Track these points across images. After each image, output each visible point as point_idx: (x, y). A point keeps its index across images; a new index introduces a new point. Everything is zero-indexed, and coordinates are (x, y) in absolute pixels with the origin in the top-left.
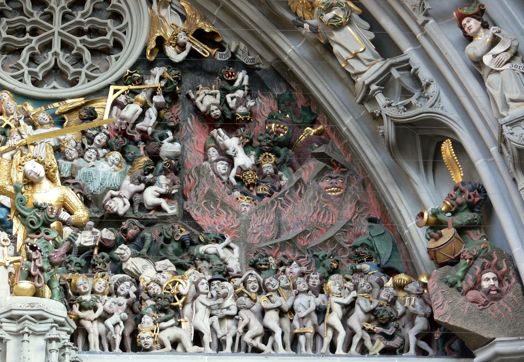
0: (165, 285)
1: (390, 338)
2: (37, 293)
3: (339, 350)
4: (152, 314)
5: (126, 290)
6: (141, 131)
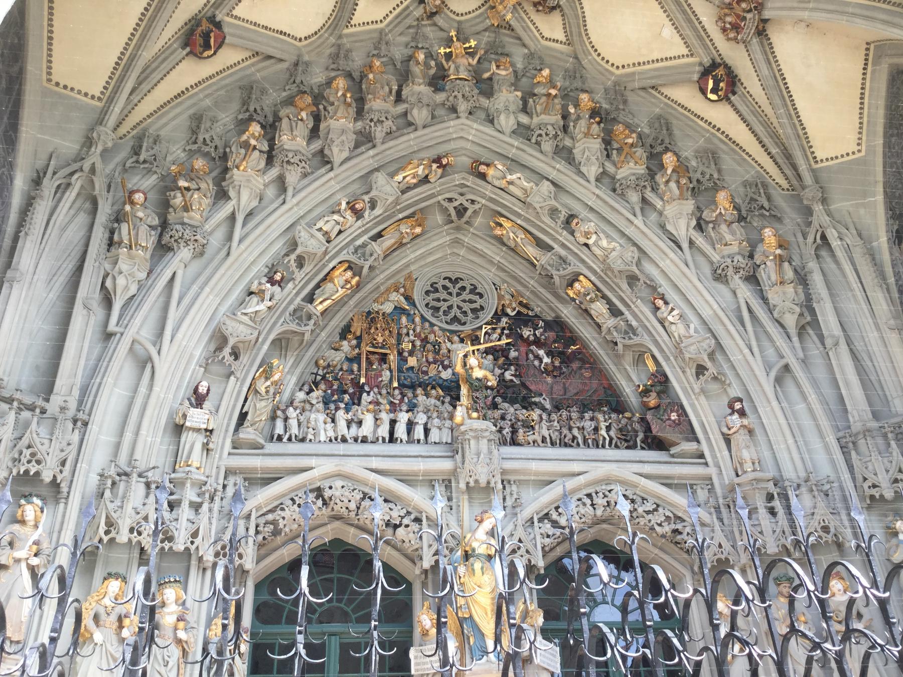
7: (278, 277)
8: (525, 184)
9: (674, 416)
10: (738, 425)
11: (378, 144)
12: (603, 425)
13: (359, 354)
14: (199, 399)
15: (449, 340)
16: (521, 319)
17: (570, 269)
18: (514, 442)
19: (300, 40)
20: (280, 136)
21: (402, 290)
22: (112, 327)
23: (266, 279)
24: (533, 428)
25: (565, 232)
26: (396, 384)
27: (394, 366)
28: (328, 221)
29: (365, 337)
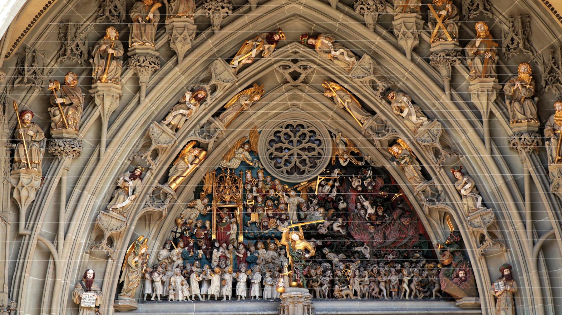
0: (343, 272)
1: (426, 292)
2: (299, 286)
3: (407, 298)
4: (339, 284)
5: (329, 275)
6: (330, 198)
7: (138, 172)
8: (348, 59)
9: (461, 274)
10: (502, 290)
11: (216, 32)
12: (406, 279)
13: (211, 211)
14: (87, 285)
17: (388, 136)
18: (331, 295)
20: (132, 43)
21: (247, 147)
22: (22, 231)
23: (128, 174)
24: (348, 283)
25: (384, 102)
26: (241, 238)
27: (240, 221)
28: (175, 116)
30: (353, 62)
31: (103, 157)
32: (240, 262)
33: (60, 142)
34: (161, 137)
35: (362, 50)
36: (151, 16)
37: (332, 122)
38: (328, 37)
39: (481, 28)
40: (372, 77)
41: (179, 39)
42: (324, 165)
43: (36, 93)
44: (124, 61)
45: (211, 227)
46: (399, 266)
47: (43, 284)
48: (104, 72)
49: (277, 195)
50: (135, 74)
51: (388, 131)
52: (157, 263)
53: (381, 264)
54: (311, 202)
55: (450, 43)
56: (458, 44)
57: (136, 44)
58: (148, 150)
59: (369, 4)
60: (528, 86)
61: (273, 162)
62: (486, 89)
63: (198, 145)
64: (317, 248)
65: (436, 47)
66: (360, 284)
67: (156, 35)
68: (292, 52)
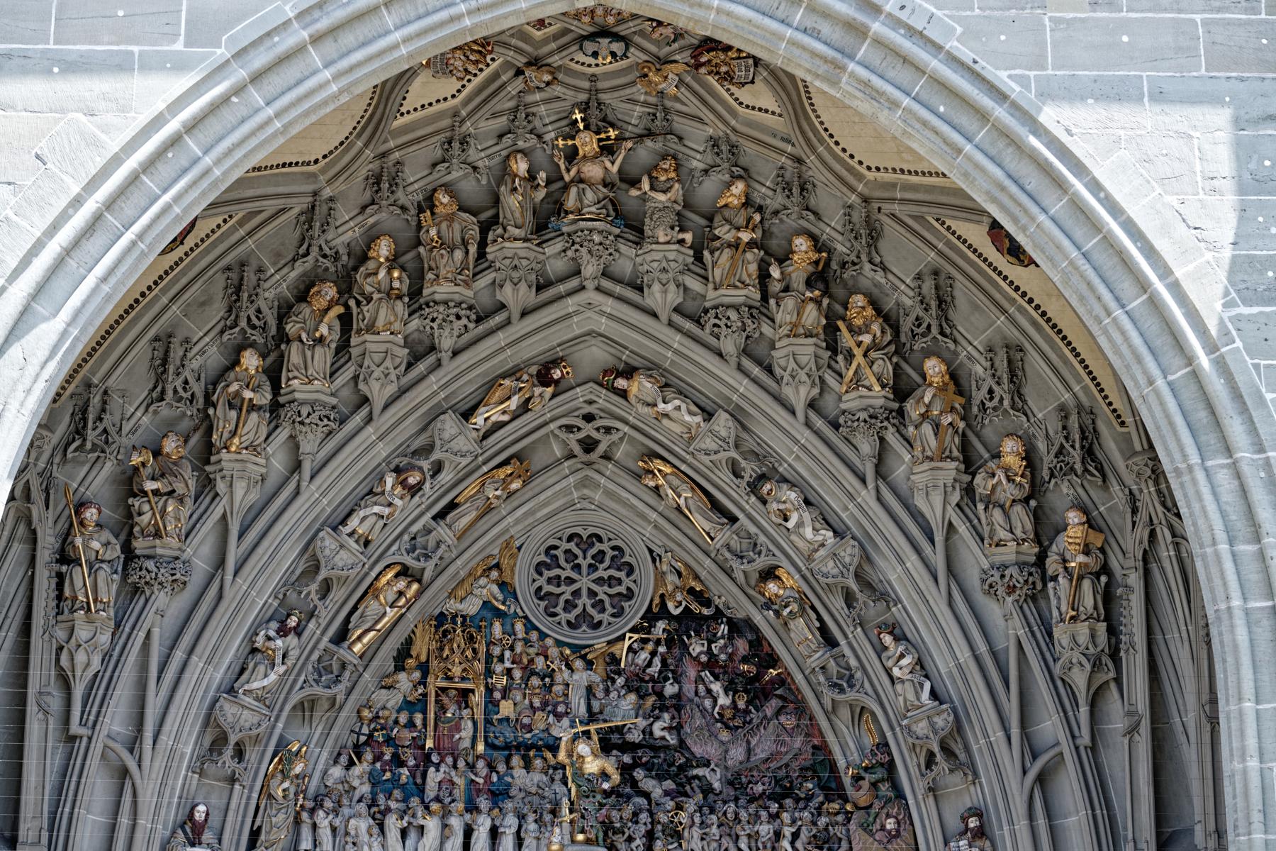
2: (588, 842)
7: (292, 622)
8: (688, 418)
9: (890, 824)
11: (445, 362)
12: (788, 831)
13: (425, 695)
15: (569, 667)
16: (689, 622)
17: (762, 562)
19: (316, 161)
20: (289, 379)
22: (75, 728)
23: (274, 625)
25: (753, 499)
26: (481, 747)
27: (480, 716)
29: (434, 663)
30: (698, 425)
31: (228, 593)
32: (479, 791)
33: (150, 564)
34: (338, 557)
35: (715, 403)
36: (324, 330)
37: (654, 532)
38: (651, 376)
39: (934, 367)
40: (734, 454)
41: (375, 375)
42: (637, 612)
43: (109, 467)
44: (271, 412)
45: (425, 725)
46: (774, 807)
47: (113, 828)
48: (234, 433)
49: (548, 666)
50: (292, 437)
51: (760, 553)
52: (323, 791)
53: (742, 802)
54: (613, 681)
55: (878, 396)
56: (891, 396)
57: (296, 381)
58: (313, 579)
59: (728, 318)
60: (1018, 479)
61: (543, 604)
62: (941, 483)
63: (404, 572)
64: (625, 770)
65: (851, 402)
66: (702, 839)
67: (333, 364)
68: (585, 402)
